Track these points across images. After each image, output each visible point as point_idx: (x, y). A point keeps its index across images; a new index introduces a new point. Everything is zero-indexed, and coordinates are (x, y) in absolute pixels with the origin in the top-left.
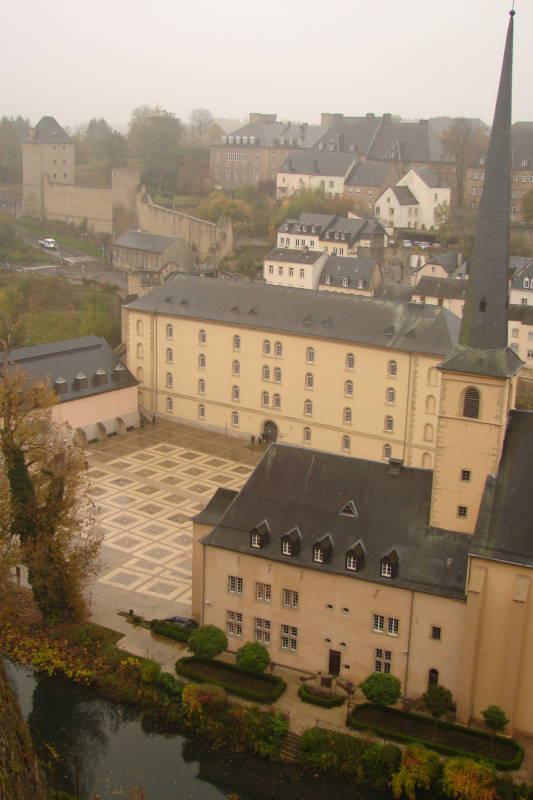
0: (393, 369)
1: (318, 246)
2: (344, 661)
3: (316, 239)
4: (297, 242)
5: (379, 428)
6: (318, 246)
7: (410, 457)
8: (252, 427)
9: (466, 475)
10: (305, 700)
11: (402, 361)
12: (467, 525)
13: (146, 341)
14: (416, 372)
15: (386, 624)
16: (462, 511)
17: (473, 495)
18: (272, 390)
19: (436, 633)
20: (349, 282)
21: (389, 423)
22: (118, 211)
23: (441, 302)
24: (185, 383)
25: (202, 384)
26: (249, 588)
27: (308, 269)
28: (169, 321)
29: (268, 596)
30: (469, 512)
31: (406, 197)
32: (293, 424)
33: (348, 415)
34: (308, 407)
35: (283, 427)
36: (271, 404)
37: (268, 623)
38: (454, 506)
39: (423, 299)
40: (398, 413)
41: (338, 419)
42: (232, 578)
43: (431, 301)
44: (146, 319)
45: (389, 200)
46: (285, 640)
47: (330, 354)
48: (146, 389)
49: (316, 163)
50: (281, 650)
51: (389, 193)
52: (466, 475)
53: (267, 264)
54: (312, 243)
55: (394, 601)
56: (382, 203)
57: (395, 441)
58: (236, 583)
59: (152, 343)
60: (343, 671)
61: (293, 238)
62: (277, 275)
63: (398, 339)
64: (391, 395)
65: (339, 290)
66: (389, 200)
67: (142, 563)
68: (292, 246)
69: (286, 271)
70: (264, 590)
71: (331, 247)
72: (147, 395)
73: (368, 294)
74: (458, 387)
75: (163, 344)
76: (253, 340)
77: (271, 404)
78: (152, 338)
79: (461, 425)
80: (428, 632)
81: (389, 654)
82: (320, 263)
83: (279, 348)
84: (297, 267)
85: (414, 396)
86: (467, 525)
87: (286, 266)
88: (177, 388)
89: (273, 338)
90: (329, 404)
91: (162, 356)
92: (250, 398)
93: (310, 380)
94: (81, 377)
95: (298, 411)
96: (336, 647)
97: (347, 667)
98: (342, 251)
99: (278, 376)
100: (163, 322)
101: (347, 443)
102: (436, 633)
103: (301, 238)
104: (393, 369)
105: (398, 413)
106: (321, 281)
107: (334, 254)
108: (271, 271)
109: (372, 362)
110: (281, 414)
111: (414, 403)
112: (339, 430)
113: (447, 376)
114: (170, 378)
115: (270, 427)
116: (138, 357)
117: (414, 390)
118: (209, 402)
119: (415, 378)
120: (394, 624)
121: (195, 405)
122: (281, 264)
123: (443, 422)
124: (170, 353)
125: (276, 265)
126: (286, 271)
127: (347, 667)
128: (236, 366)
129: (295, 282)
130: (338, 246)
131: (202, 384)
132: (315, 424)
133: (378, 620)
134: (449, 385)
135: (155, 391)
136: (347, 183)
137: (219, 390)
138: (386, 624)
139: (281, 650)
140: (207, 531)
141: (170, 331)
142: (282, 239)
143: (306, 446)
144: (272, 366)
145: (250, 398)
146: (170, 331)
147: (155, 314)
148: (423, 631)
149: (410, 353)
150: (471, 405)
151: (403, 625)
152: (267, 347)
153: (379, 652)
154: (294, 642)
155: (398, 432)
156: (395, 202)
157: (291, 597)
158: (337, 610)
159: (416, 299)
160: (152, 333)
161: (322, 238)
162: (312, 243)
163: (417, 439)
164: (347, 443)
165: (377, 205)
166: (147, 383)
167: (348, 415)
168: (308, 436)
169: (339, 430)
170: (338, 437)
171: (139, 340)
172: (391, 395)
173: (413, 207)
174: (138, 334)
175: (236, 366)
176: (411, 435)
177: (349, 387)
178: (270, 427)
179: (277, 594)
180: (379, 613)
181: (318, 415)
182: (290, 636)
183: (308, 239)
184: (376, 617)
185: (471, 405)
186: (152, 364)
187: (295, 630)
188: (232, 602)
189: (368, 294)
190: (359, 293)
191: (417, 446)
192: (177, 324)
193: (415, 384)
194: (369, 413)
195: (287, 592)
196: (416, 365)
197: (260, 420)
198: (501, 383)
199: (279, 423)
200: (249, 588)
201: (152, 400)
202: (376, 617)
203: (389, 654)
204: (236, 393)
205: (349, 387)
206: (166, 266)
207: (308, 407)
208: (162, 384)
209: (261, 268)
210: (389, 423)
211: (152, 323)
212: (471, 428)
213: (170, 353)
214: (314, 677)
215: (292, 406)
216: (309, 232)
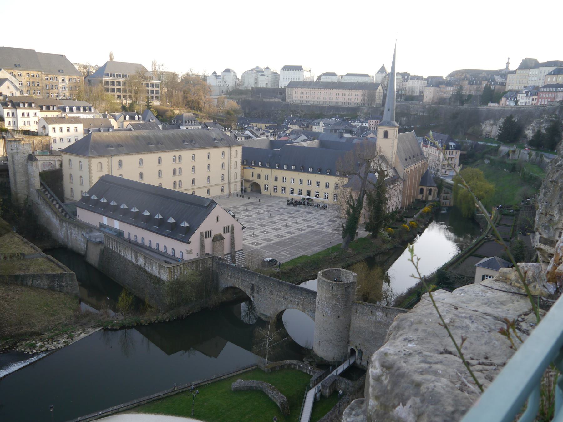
11: (226, 150)
18: (177, 179)
41: (205, 183)
45: (8, 88)
57: (226, 183)
64: (223, 166)
66: (8, 88)
76: (167, 157)
83: (180, 159)
89: (177, 154)
122: (61, 125)
125: (57, 127)
132: (197, 188)
142: (8, 114)
149: (230, 146)
152: (174, 160)
155: (226, 180)
163: (232, 180)
169: (206, 187)
170: (206, 190)
172: (223, 166)
191: (233, 182)
196: (231, 151)
210: (223, 178)
211: (108, 162)
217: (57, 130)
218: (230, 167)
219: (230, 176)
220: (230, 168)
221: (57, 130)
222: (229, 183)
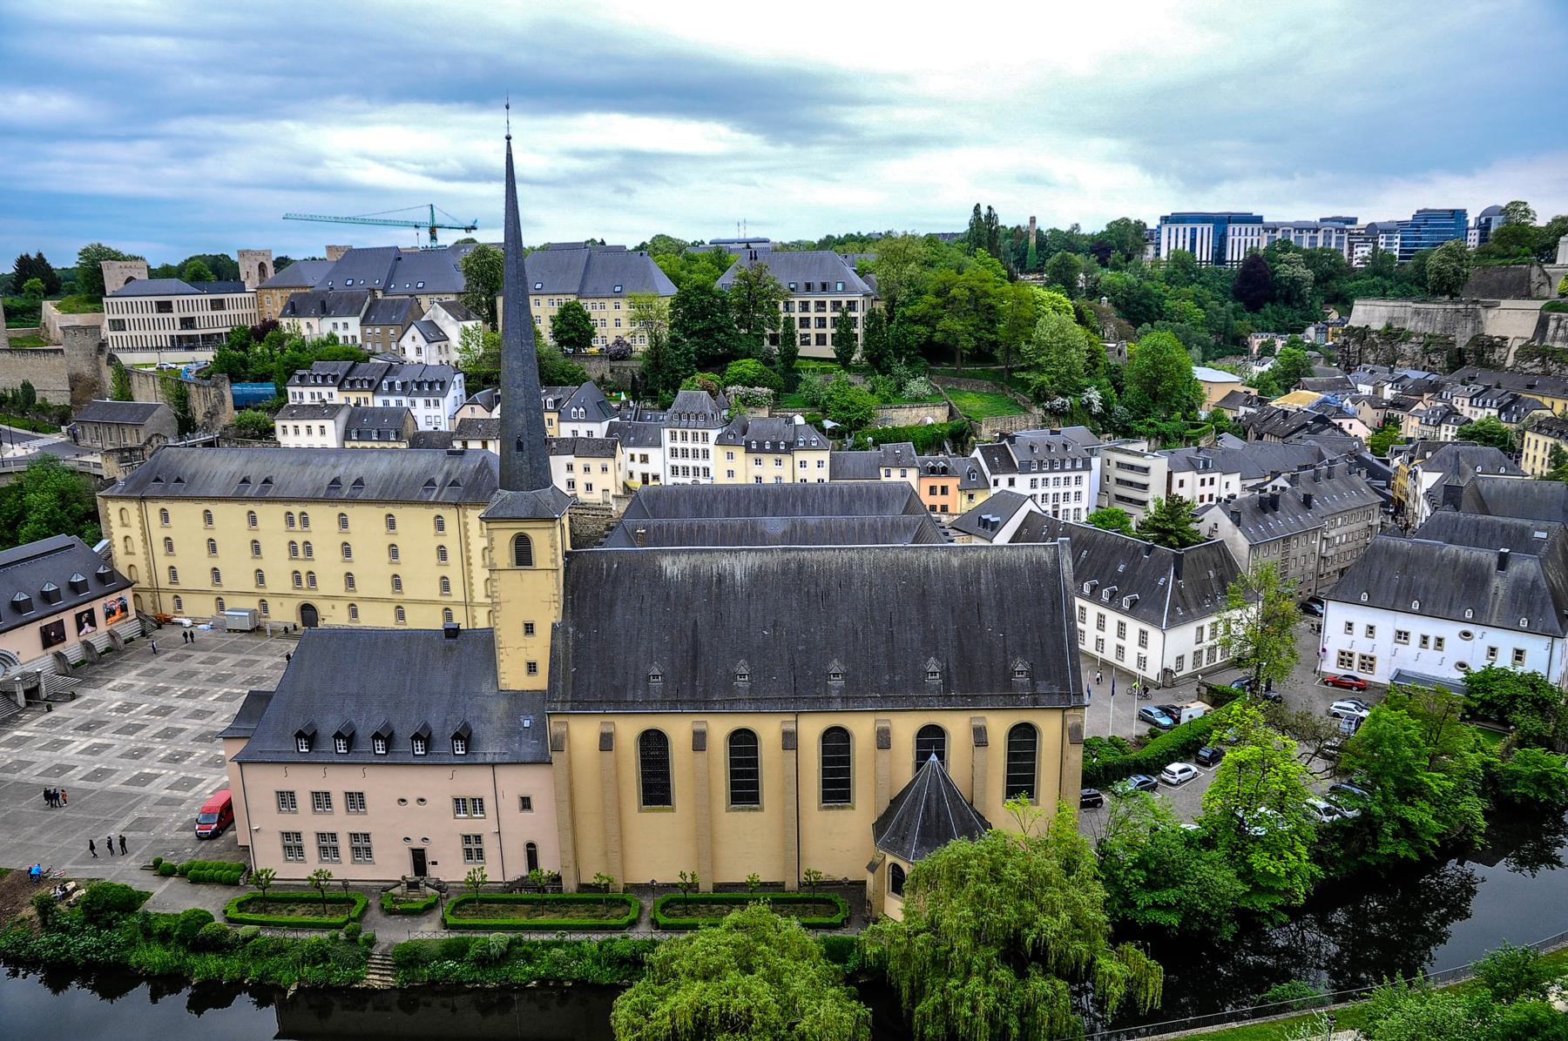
0: (440, 524)
1: (338, 398)
2: (429, 859)
3: (334, 390)
4: (313, 395)
5: (434, 592)
6: (338, 398)
7: (474, 617)
8: (284, 613)
9: (529, 628)
10: (391, 912)
11: (450, 515)
12: (540, 681)
13: (135, 533)
14: (466, 524)
15: (469, 806)
16: (532, 668)
17: (539, 648)
18: (303, 568)
19: (526, 803)
20: (379, 434)
21: (445, 584)
22: (74, 380)
23: (485, 445)
24: (194, 573)
25: (216, 573)
26: (304, 801)
27: (329, 425)
28: (162, 505)
29: (329, 805)
30: (539, 667)
31: (434, 334)
32: (335, 603)
33: (397, 582)
34: (350, 580)
35: (323, 608)
36: (304, 584)
37: (333, 836)
38: (522, 663)
39: (465, 444)
40: (454, 572)
41: (386, 590)
42: (281, 794)
43: (475, 445)
44: (132, 508)
46: (356, 850)
47: (367, 521)
48: (144, 590)
49: (323, 303)
50: (354, 862)
51: (413, 330)
52: (529, 628)
53: (278, 424)
54: (331, 395)
55: (473, 782)
56: (406, 342)
57: (456, 603)
58: (286, 799)
59: (144, 534)
60: (430, 868)
61: (307, 391)
62: (293, 435)
63: (440, 491)
64: (442, 553)
65: (369, 445)
67: (165, 801)
68: (307, 401)
69: (303, 430)
70: (321, 800)
71: (353, 398)
72: (146, 598)
73: (404, 446)
74: (504, 538)
75: (158, 534)
76: (271, 516)
77: (304, 584)
78: (143, 528)
79: (515, 575)
80: (517, 804)
81: (478, 838)
82: (342, 417)
83: (305, 520)
84: (315, 424)
85: (468, 551)
86: (540, 681)
87: (302, 425)
88: (185, 582)
89: (296, 509)
90: (373, 577)
91: (159, 548)
92: (279, 581)
93: (347, 550)
94: (49, 588)
95: (339, 588)
96: (418, 845)
97: (435, 863)
98: (366, 400)
99: (308, 549)
100: (153, 509)
101: (400, 614)
102: (526, 803)
103: (315, 390)
104: (440, 524)
105: (454, 572)
106: (347, 436)
107: (357, 405)
108: (285, 432)
109: (415, 523)
110: (322, 592)
111: (469, 558)
112: (389, 600)
113: (491, 526)
114: (173, 572)
115: (308, 613)
116: (128, 553)
117: (468, 544)
118: (229, 593)
119: (467, 531)
120: (478, 804)
121: (212, 600)
122: (296, 423)
123: (495, 576)
124: (169, 544)
125: (290, 424)
126: (303, 430)
127: (435, 863)
128: (256, 548)
129: (316, 441)
130: (362, 395)
131: (216, 573)
133: (460, 804)
134: (495, 534)
135: (156, 591)
136: (363, 323)
137: (238, 575)
138: (469, 806)
139: (354, 862)
140: (238, 747)
141: (165, 515)
142: (294, 394)
143: (355, 625)
144: (299, 539)
145: (279, 581)
146: (165, 515)
147: (143, 499)
148: (511, 803)
149: (457, 505)
150: (523, 554)
151: (489, 804)
153: (467, 838)
154: (368, 849)
155: (457, 592)
156: (421, 341)
157: (356, 800)
158: (412, 801)
159: (458, 445)
160: (142, 522)
161: (340, 387)
162: (331, 395)
163: (479, 596)
164: (400, 614)
165: (402, 343)
166: (144, 582)
167: (397, 582)
168: (354, 612)
169: (389, 600)
171: (126, 532)
172: (442, 553)
173: (442, 344)
174: (124, 525)
175: (256, 548)
176: (471, 591)
177: (394, 551)
178: (308, 613)
179: (338, 801)
180: (460, 795)
181: (362, 589)
182: (362, 846)
183: (325, 391)
184: (457, 800)
185: (523, 554)
186: (147, 559)
187: (367, 836)
188: (290, 822)
189: (404, 446)
190: (392, 445)
191: (481, 605)
192: (174, 508)
193: (467, 537)
194: (421, 579)
195: (349, 795)
196: (465, 516)
197: (297, 602)
198: (550, 525)
199: (315, 603)
200: (304, 801)
201: (153, 602)
202: (457, 800)
203: (478, 838)
204: (260, 577)
205: (394, 551)
206: (150, 440)
207: (350, 580)
208: (164, 580)
209: (273, 430)
210: (445, 584)
212: (528, 575)
213: (169, 544)
214: (398, 884)
215: (329, 582)
216: (324, 383)
217: (290, 430)
218: (467, 562)
219: (468, 583)
220: (469, 564)
221: (290, 430)
222: (468, 604)
